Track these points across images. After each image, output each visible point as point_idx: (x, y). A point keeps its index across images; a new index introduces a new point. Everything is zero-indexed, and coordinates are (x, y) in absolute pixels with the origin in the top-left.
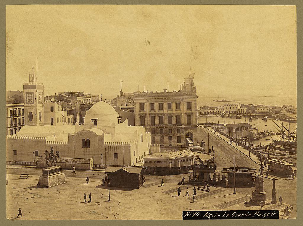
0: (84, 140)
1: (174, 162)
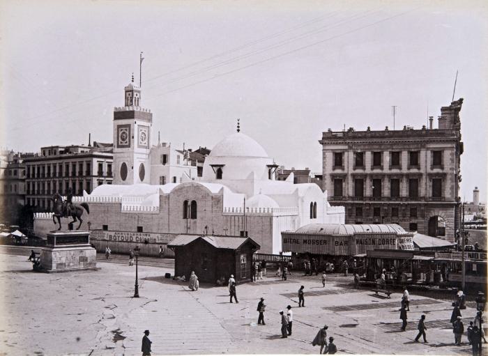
0: (186, 203)
1: (346, 243)
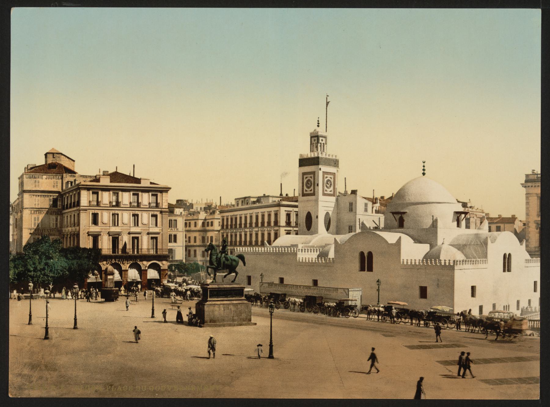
0: (362, 254)
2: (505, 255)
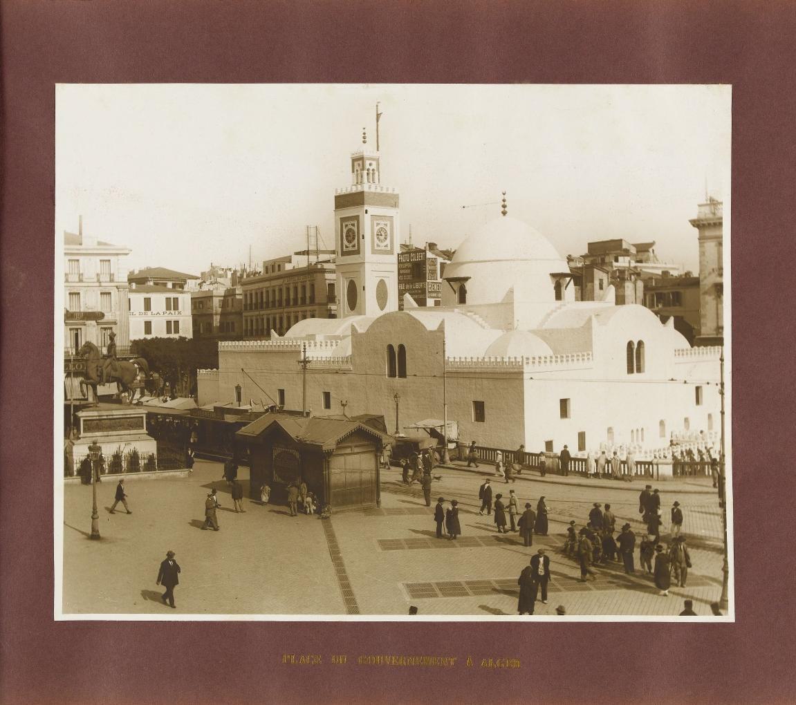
0: (390, 347)
2: (630, 344)
